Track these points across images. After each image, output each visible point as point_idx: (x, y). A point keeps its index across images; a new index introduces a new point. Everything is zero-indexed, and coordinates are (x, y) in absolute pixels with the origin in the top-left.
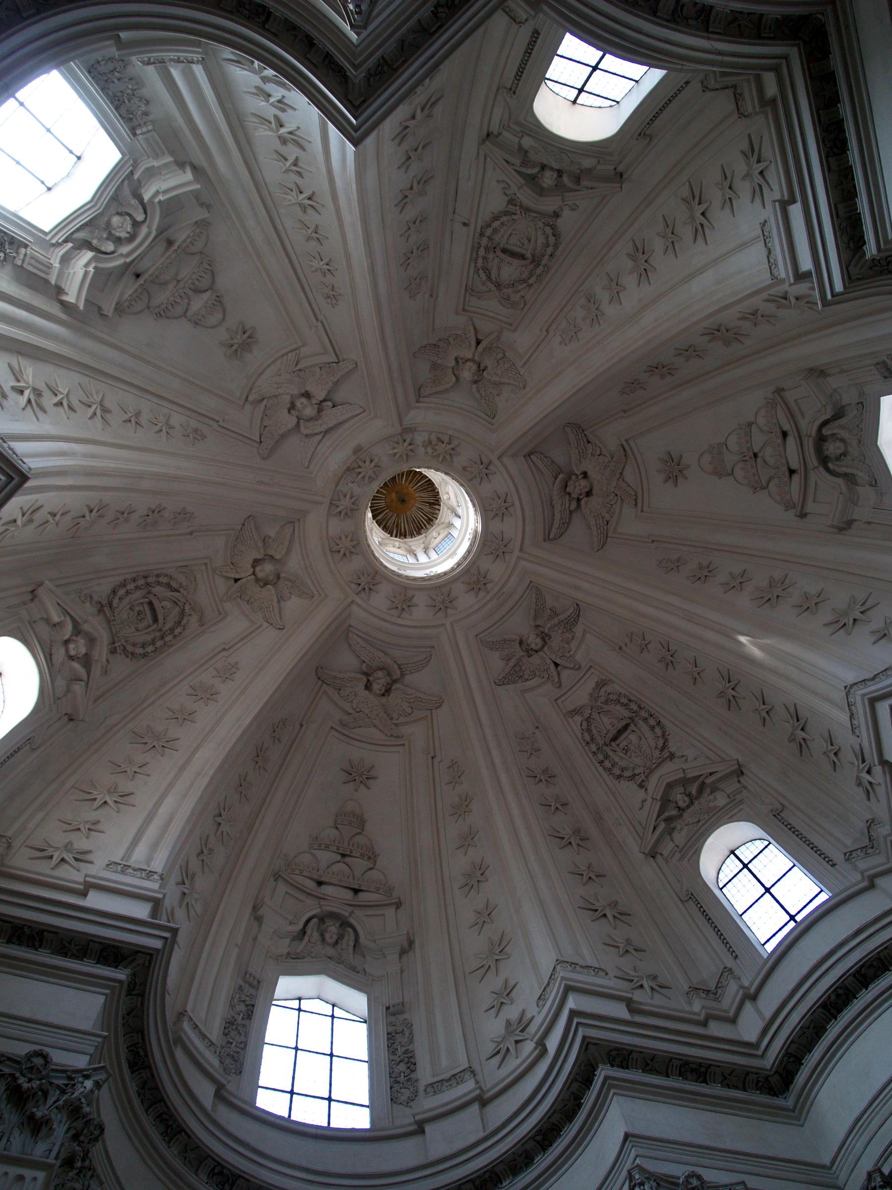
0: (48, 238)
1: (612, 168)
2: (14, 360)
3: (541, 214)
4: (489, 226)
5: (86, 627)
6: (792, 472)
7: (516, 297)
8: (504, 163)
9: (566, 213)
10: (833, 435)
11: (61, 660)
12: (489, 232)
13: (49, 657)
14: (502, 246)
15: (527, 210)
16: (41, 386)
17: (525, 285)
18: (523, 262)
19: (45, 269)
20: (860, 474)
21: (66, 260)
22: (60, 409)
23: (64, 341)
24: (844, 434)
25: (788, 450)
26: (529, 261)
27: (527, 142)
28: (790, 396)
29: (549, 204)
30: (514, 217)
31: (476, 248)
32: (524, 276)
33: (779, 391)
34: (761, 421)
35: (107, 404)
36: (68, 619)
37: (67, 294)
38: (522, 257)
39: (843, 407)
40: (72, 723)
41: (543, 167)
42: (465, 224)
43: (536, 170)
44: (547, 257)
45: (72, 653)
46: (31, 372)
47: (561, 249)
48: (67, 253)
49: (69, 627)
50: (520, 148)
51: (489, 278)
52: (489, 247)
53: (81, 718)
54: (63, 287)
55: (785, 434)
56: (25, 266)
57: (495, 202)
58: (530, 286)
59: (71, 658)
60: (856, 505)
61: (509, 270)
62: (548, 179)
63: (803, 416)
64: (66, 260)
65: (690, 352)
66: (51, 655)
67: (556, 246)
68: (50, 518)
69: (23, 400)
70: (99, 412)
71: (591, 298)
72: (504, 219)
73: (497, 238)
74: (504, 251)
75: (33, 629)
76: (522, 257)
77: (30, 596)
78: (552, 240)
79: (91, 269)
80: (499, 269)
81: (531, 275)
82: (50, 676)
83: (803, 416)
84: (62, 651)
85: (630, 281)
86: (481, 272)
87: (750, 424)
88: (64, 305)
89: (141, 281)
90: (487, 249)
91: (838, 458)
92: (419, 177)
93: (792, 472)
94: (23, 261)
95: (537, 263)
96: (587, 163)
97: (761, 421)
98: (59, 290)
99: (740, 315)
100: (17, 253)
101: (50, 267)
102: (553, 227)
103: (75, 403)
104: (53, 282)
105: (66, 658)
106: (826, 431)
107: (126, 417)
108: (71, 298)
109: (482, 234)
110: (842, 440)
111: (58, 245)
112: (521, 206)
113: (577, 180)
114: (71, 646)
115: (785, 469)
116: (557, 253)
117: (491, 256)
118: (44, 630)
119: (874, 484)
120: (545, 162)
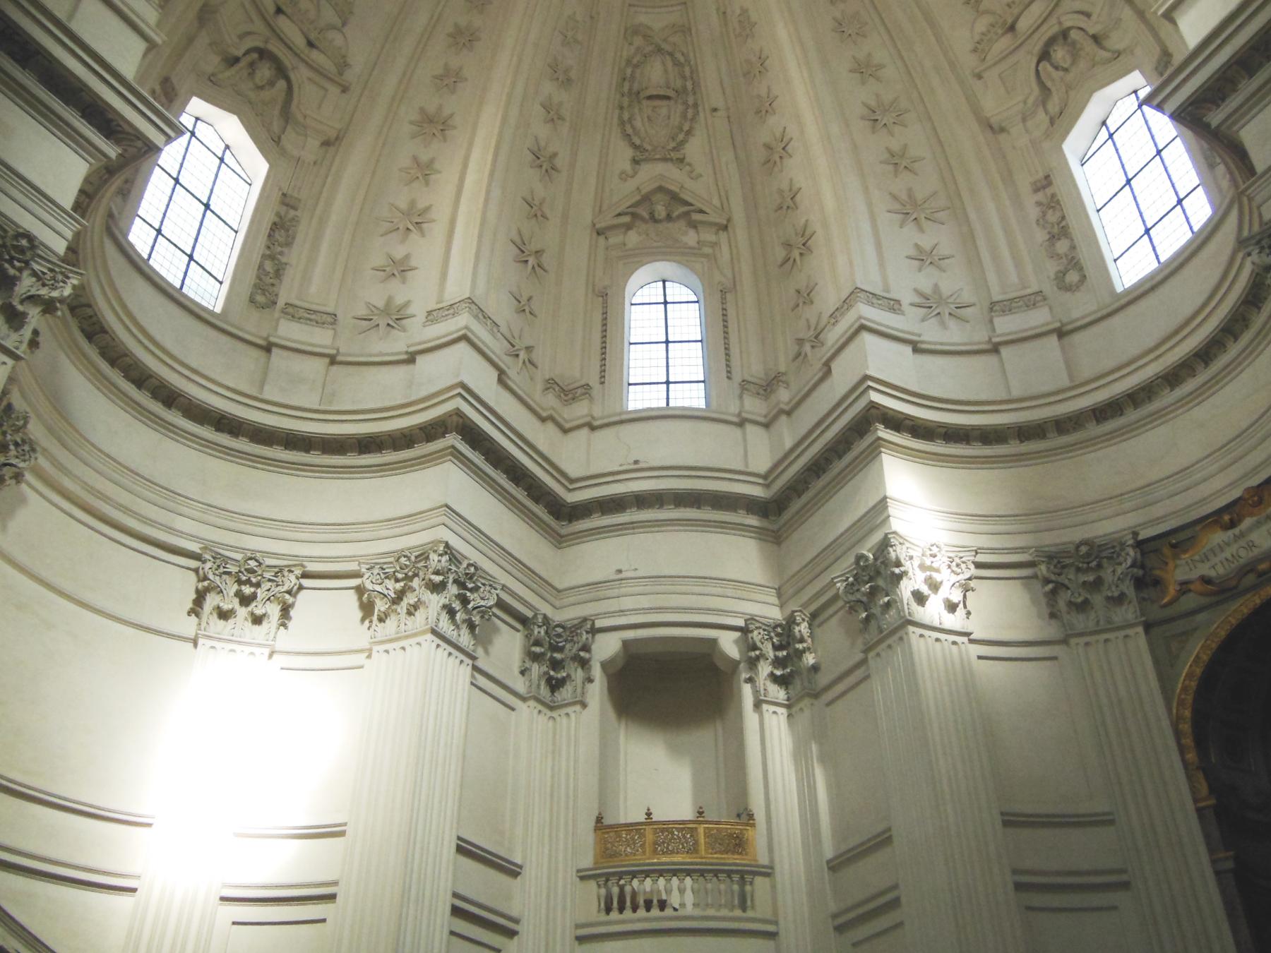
1: (612, 240)
3: (647, 160)
4: (692, 120)
6: (279, 11)
7: (638, 41)
8: (704, 208)
9: (627, 167)
10: (271, 83)
12: (690, 115)
14: (672, 102)
15: (665, 160)
17: (635, 61)
18: (648, 93)
20: (227, 74)
24: (267, 94)
25: (299, 33)
26: (642, 95)
27: (691, 238)
28: (334, 90)
29: (650, 174)
30: (672, 145)
31: (696, 85)
32: (638, 71)
33: (345, 89)
34: (338, 39)
38: (650, 98)
39: (287, 122)
41: (669, 218)
42: (715, 110)
43: (675, 214)
44: (626, 104)
47: (615, 120)
50: (695, 227)
51: (671, 54)
52: (683, 94)
55: (311, 44)
57: (695, 149)
58: (629, 62)
60: (210, 45)
61: (656, 74)
62: (661, 211)
63: (309, 79)
65: (450, 80)
67: (622, 123)
71: (567, 83)
72: (681, 137)
73: (680, 108)
74: (668, 98)
76: (650, 98)
78: (630, 131)
80: (666, 71)
81: (633, 76)
83: (309, 79)
85: (542, 131)
86: (682, 59)
87: (344, 24)
90: (685, 88)
91: (252, 65)
92: (776, 169)
93: (279, 11)
95: (633, 95)
96: (633, 238)
97: (338, 39)
99: (437, 166)
102: (636, 147)
106: (282, 84)
109: (696, 105)
110: (262, 88)
112: (671, 160)
113: (635, 216)
115: (288, 10)
116: (617, 112)
117: (678, 83)
119: (212, 80)
120: (670, 225)
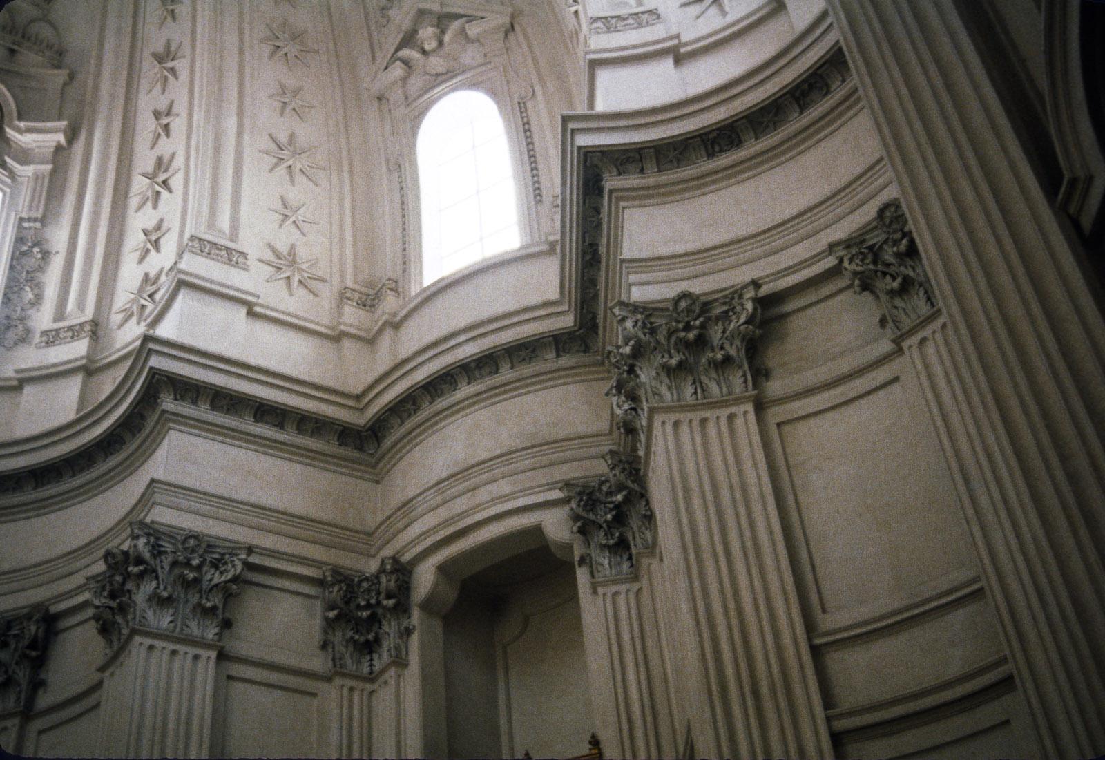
0: (8, 190)
2: (134, 201)
5: (407, 25)
11: (441, 61)
13: (440, 78)
16: (150, 168)
19: (40, 181)
21: (25, 157)
22: (172, 126)
23: (108, 126)
35: (160, 48)
36: (400, 54)
37: (59, 142)
40: (517, 28)
45: (434, 44)
46: (139, 184)
48: (14, 159)
49: (406, 53)
53: (507, 20)
54: (52, 149)
56: (39, 215)
59: (441, 43)
64: (25, 157)
66: (438, 75)
68: (289, 109)
69: (164, 194)
70: (170, 64)
75: (415, 100)
77: (384, 101)
79: (22, 124)
82: (463, 72)
84: (433, 60)
88: (72, 134)
89: (15, 47)
94: (35, 220)
98: (59, 148)
100: (30, 228)
101: (37, 177)
103: (162, 105)
104: (49, 167)
105: (441, 53)
107: (169, 19)
108: (60, 138)
111: (12, 175)
114: (427, 47)
118: (416, 82)
